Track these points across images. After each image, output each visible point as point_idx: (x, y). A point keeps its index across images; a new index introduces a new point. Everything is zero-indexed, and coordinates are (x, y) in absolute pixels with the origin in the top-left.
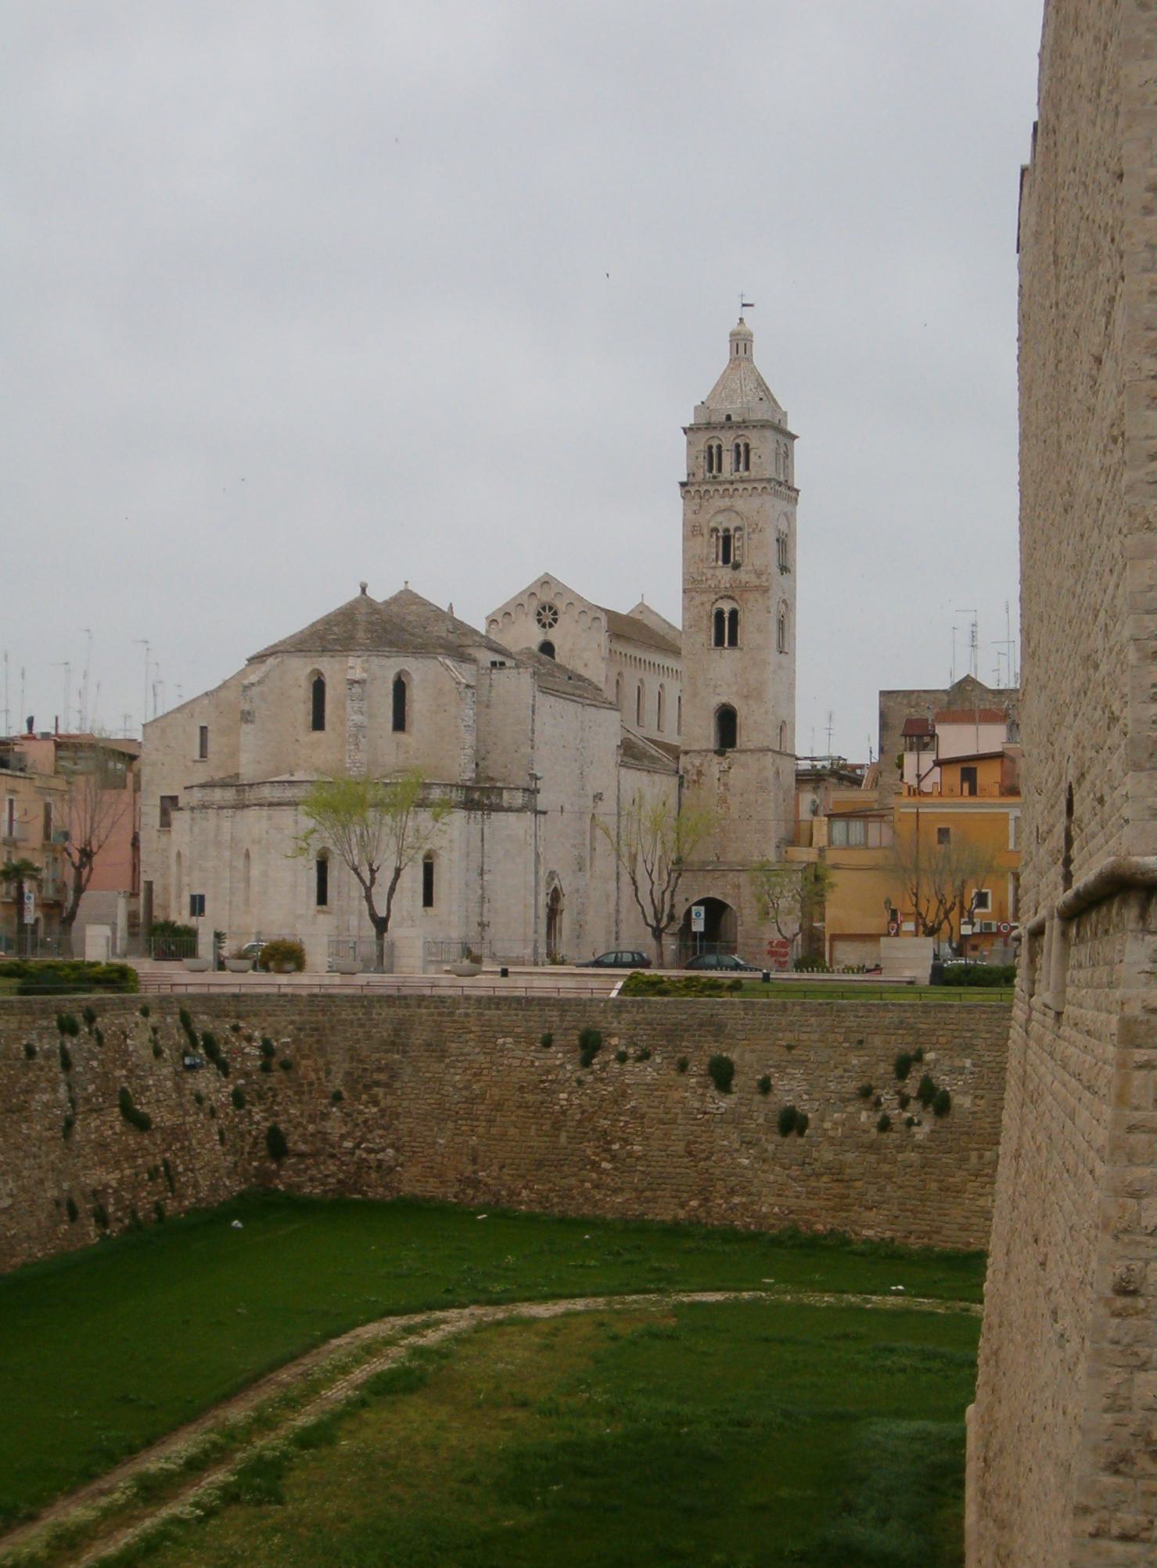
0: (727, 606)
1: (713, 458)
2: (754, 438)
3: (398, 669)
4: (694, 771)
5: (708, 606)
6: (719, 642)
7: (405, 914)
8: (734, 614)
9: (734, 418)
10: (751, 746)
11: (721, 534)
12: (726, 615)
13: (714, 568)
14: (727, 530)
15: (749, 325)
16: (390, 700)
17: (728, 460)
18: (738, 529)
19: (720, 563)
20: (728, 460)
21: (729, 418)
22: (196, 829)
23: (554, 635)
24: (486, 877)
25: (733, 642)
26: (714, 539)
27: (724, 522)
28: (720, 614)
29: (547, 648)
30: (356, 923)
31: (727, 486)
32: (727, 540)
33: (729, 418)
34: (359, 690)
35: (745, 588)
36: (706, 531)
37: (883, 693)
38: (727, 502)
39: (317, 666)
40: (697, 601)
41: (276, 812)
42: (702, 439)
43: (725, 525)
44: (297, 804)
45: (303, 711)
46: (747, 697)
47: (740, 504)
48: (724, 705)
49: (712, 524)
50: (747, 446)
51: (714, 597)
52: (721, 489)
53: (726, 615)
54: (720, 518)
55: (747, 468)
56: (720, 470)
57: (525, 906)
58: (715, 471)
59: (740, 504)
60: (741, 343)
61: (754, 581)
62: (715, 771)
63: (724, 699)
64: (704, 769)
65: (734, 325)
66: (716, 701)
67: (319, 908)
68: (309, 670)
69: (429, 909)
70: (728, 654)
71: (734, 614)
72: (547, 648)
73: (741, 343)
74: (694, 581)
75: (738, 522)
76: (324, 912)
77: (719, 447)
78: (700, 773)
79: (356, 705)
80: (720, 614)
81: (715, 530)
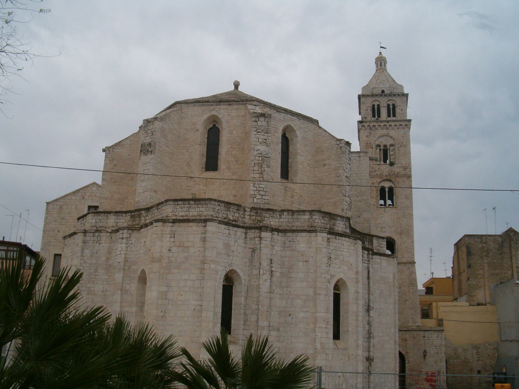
0: (387, 185)
1: (376, 111)
2: (398, 101)
3: (286, 124)
7: (318, 346)
8: (391, 189)
9: (386, 92)
11: (382, 148)
12: (387, 190)
14: (385, 146)
15: (384, 55)
16: (279, 147)
17: (384, 112)
18: (392, 145)
19: (382, 163)
20: (384, 112)
21: (383, 91)
22: (87, 252)
24: (372, 313)
26: (378, 150)
27: (383, 141)
28: (383, 189)
31: (385, 123)
33: (383, 91)
34: (264, 123)
35: (398, 175)
36: (374, 146)
38: (385, 132)
39: (214, 113)
41: (180, 228)
42: (369, 102)
43: (384, 143)
44: (205, 221)
45: (198, 152)
46: (401, 234)
47: (392, 133)
49: (377, 143)
50: (394, 105)
51: (379, 180)
52: (382, 124)
53: (387, 190)
54: (382, 140)
55: (394, 115)
56: (379, 116)
58: (376, 117)
59: (392, 133)
60: (381, 62)
61: (402, 172)
65: (377, 55)
69: (337, 342)
71: (391, 189)
73: (381, 62)
75: (392, 142)
77: (379, 106)
79: (261, 137)
80: (383, 189)
81: (378, 146)
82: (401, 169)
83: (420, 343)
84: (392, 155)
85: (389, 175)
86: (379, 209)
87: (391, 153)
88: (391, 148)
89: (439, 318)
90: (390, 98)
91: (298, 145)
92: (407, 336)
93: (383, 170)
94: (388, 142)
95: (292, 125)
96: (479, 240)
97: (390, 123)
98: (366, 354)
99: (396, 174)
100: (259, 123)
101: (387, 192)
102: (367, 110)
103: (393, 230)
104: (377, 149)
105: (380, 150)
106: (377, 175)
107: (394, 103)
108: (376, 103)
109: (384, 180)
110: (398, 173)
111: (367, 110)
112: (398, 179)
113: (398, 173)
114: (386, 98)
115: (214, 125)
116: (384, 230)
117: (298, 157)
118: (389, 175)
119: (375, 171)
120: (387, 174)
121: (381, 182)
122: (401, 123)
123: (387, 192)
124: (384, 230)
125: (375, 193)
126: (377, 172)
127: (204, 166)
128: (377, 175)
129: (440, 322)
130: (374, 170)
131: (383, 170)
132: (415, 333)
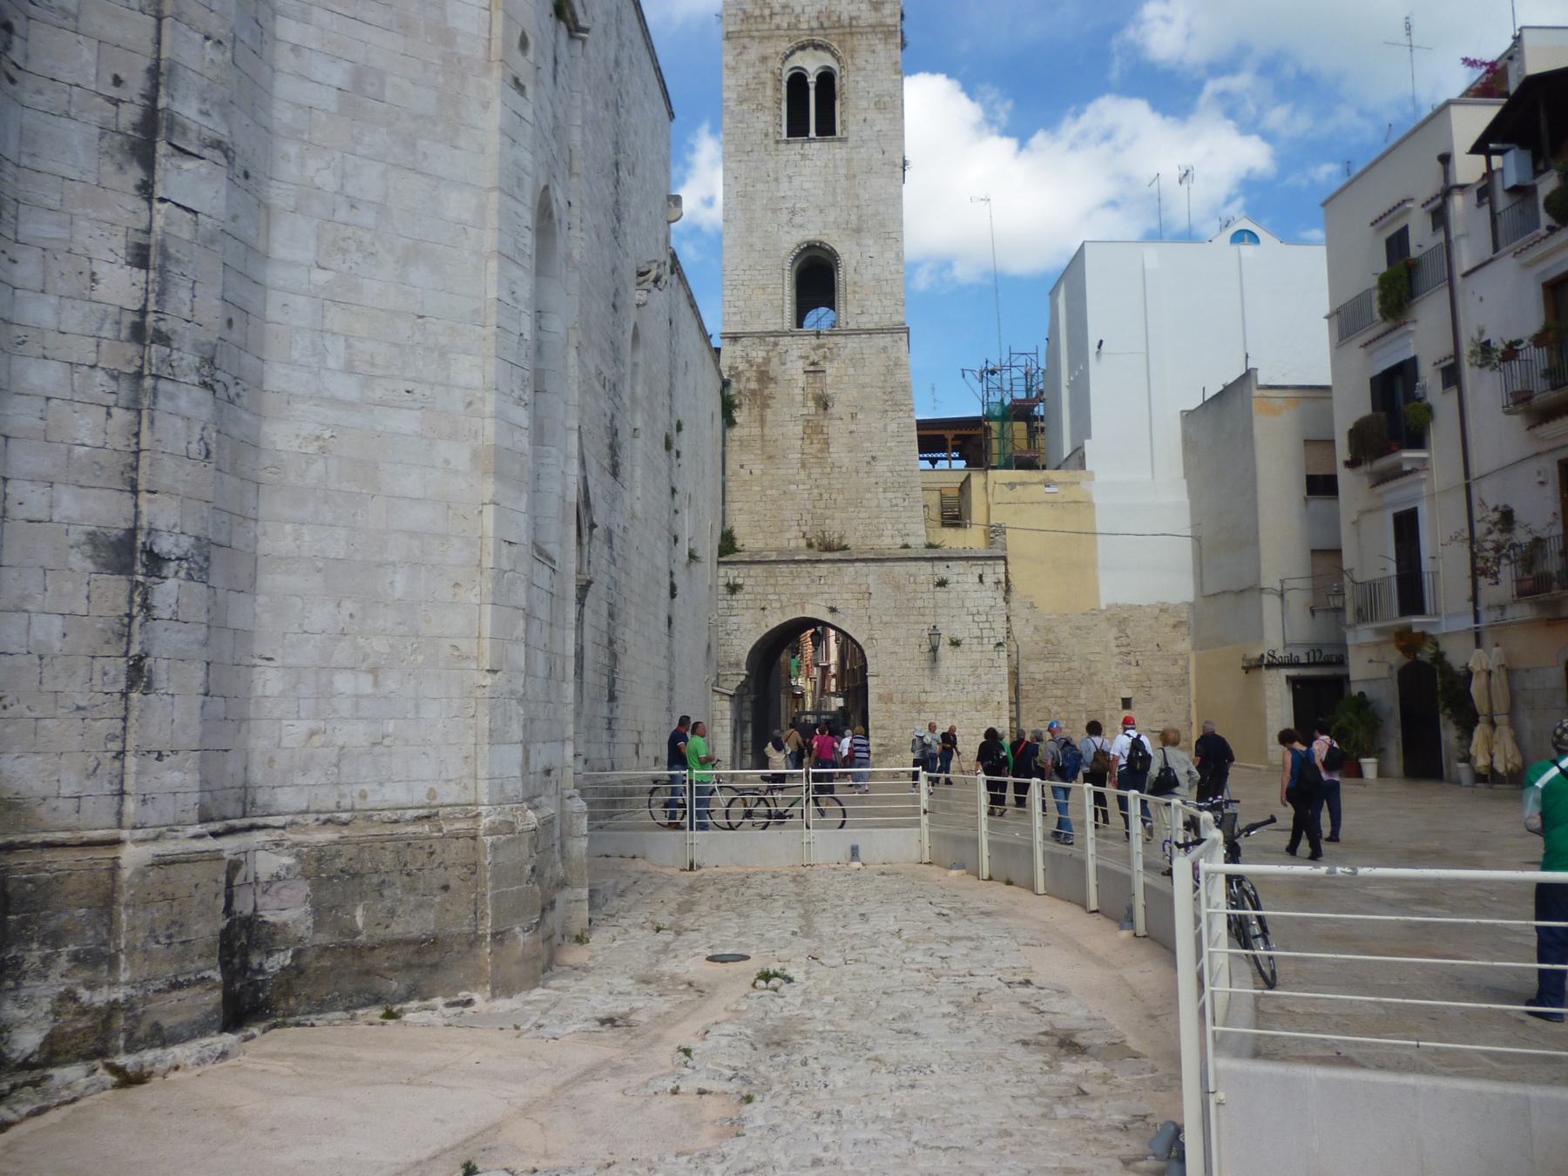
0: (812, 64)
4: (752, 374)
5: (775, 64)
6: (797, 128)
8: (827, 80)
10: (866, 322)
12: (812, 80)
25: (827, 128)
28: (797, 82)
40: (754, 52)
46: (858, 230)
48: (811, 247)
51: (784, 46)
53: (812, 80)
62: (795, 369)
63: (811, 234)
64: (774, 368)
66: (790, 241)
70: (816, 150)
71: (827, 80)
74: (747, 17)
78: (764, 377)
80: (797, 82)
83: (919, 603)
85: (822, 27)
86: (782, 146)
89: (992, 522)
92: (870, 580)
98: (106, 510)
99: (846, 22)
101: (812, 87)
106: (778, 28)
109: (803, 48)
110: (851, 19)
113: (851, 19)
116: (798, 219)
118: (822, 27)
119: (772, 15)
120: (815, 24)
121: (792, 53)
123: (812, 87)
125: (769, 92)
126: (777, 19)
128: (778, 28)
129: (994, 532)
130: (767, 12)
132: (899, 569)
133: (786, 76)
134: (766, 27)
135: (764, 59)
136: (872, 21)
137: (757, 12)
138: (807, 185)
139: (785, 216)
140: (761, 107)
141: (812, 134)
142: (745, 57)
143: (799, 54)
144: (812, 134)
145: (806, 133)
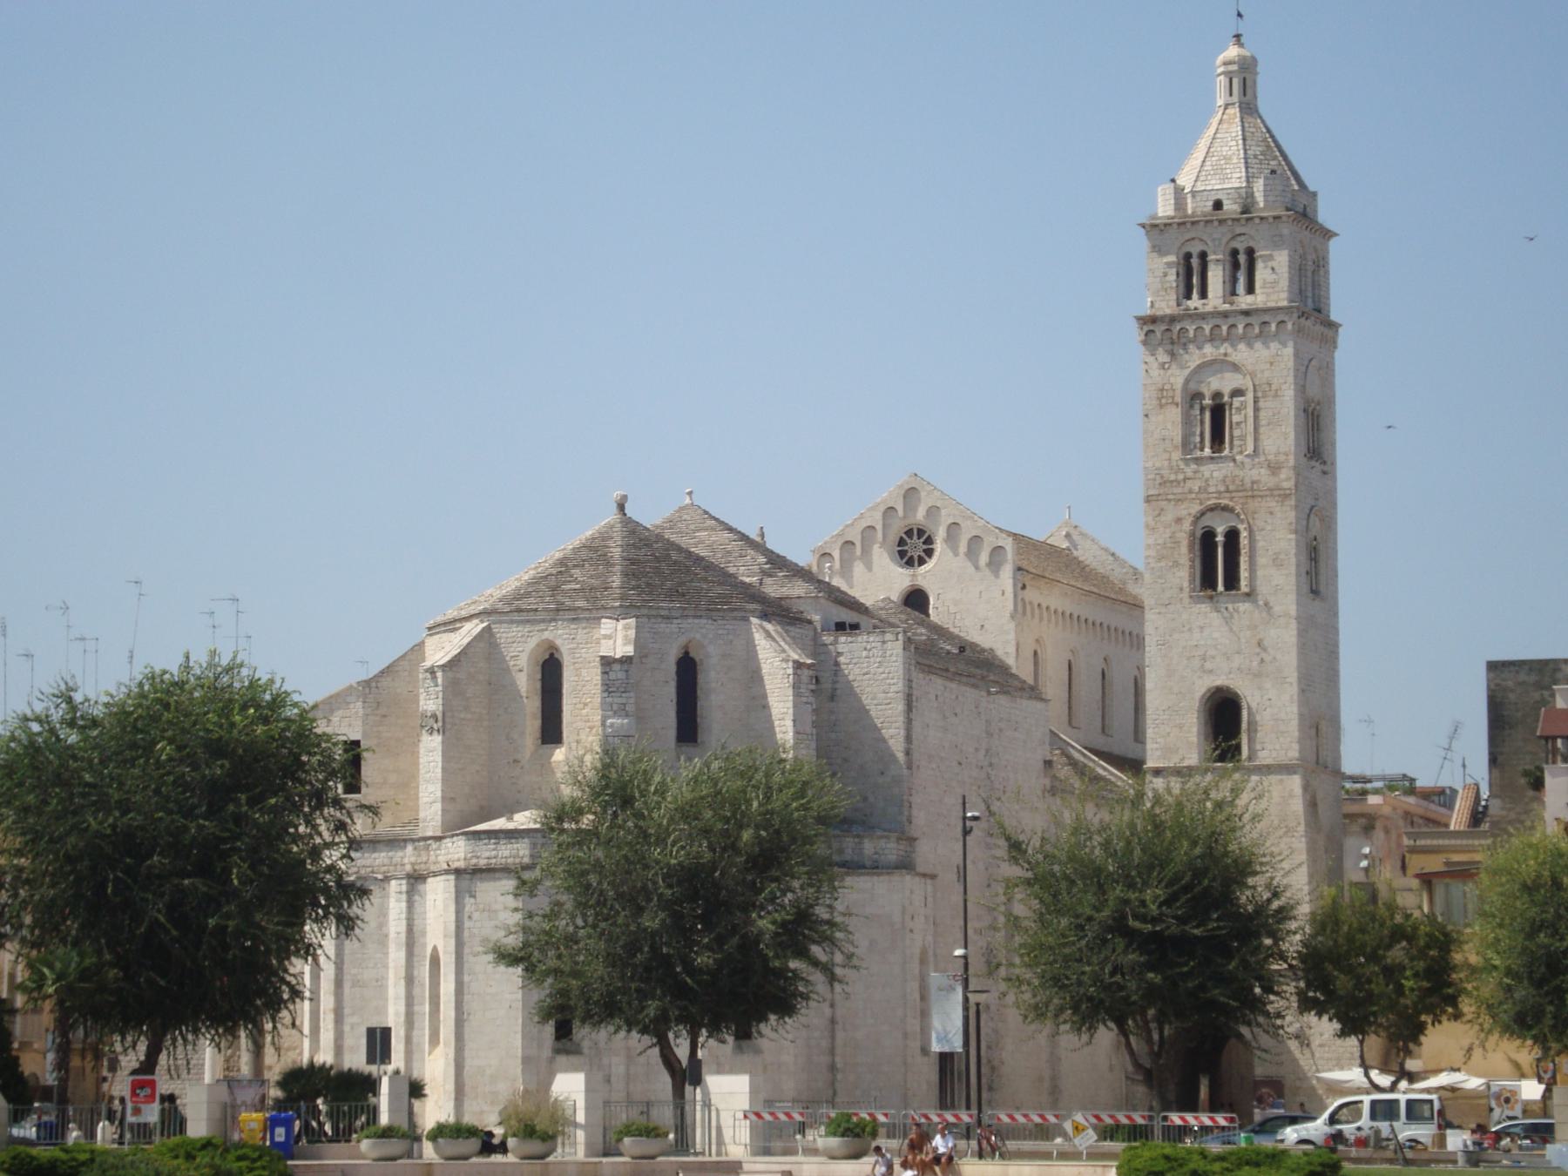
6: (1208, 581)
11: (1207, 402)
12: (1220, 539)
13: (1198, 460)
14: (1217, 395)
16: (671, 691)
17: (1216, 277)
18: (1237, 393)
21: (1218, 205)
23: (927, 576)
25: (1232, 582)
26: (1197, 407)
28: (1208, 537)
29: (916, 600)
30: (621, 1069)
31: (1218, 321)
32: (1218, 413)
33: (1218, 205)
34: (621, 675)
37: (1493, 666)
39: (546, 635)
40: (1169, 517)
48: (1219, 691)
51: (1196, 508)
53: (1220, 539)
55: (1250, 289)
57: (905, 1036)
63: (1219, 682)
67: (560, 1045)
68: (532, 643)
69: (745, 1043)
71: (1232, 536)
72: (916, 600)
76: (568, 1052)
77: (1203, 256)
80: (1208, 537)
82: (1263, 471)
84: (1238, 424)
85: (1228, 491)
87: (1236, 418)
88: (1237, 401)
90: (1239, 230)
91: (713, 674)
93: (1207, 474)
94: (1223, 383)
95: (698, 636)
96: (1533, 678)
97: (1231, 321)
100: (612, 676)
102: (1165, 275)
103: (1235, 664)
104: (1192, 407)
105: (1202, 409)
107: (1251, 244)
108: (1195, 249)
110: (1253, 483)
111: (1165, 275)
112: (1252, 504)
113: (1253, 483)
114: (1224, 229)
115: (552, 655)
117: (713, 697)
119: (1185, 480)
122: (1266, 318)
124: (1208, 665)
126: (1189, 484)
127: (538, 735)
128: (1191, 492)
131: (1207, 474)
133: (1199, 533)
134: (1179, 490)
135: (1179, 520)
136: (1270, 485)
137: (1173, 477)
138: (1216, 635)
139: (1196, 663)
140: (1176, 564)
141: (1220, 587)
142: (1163, 518)
143: (1209, 515)
144: (1220, 587)
145: (1214, 586)
